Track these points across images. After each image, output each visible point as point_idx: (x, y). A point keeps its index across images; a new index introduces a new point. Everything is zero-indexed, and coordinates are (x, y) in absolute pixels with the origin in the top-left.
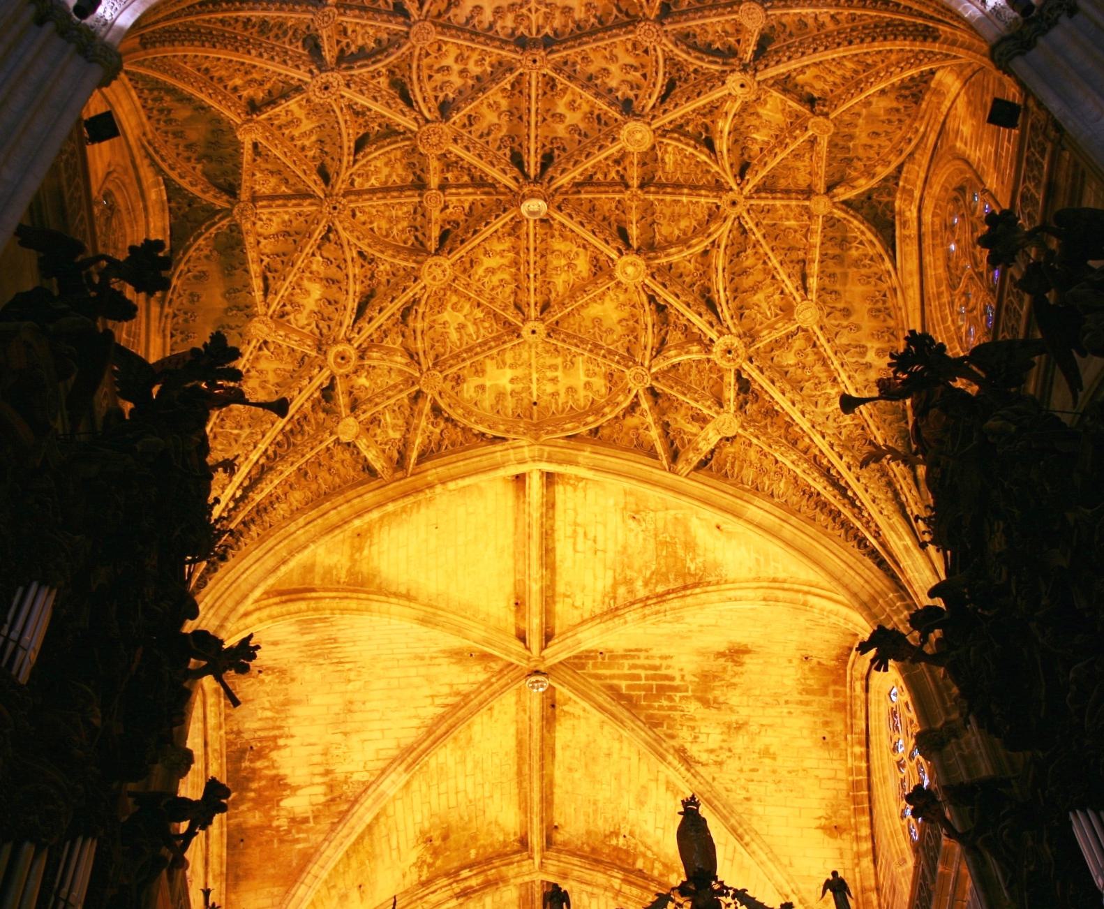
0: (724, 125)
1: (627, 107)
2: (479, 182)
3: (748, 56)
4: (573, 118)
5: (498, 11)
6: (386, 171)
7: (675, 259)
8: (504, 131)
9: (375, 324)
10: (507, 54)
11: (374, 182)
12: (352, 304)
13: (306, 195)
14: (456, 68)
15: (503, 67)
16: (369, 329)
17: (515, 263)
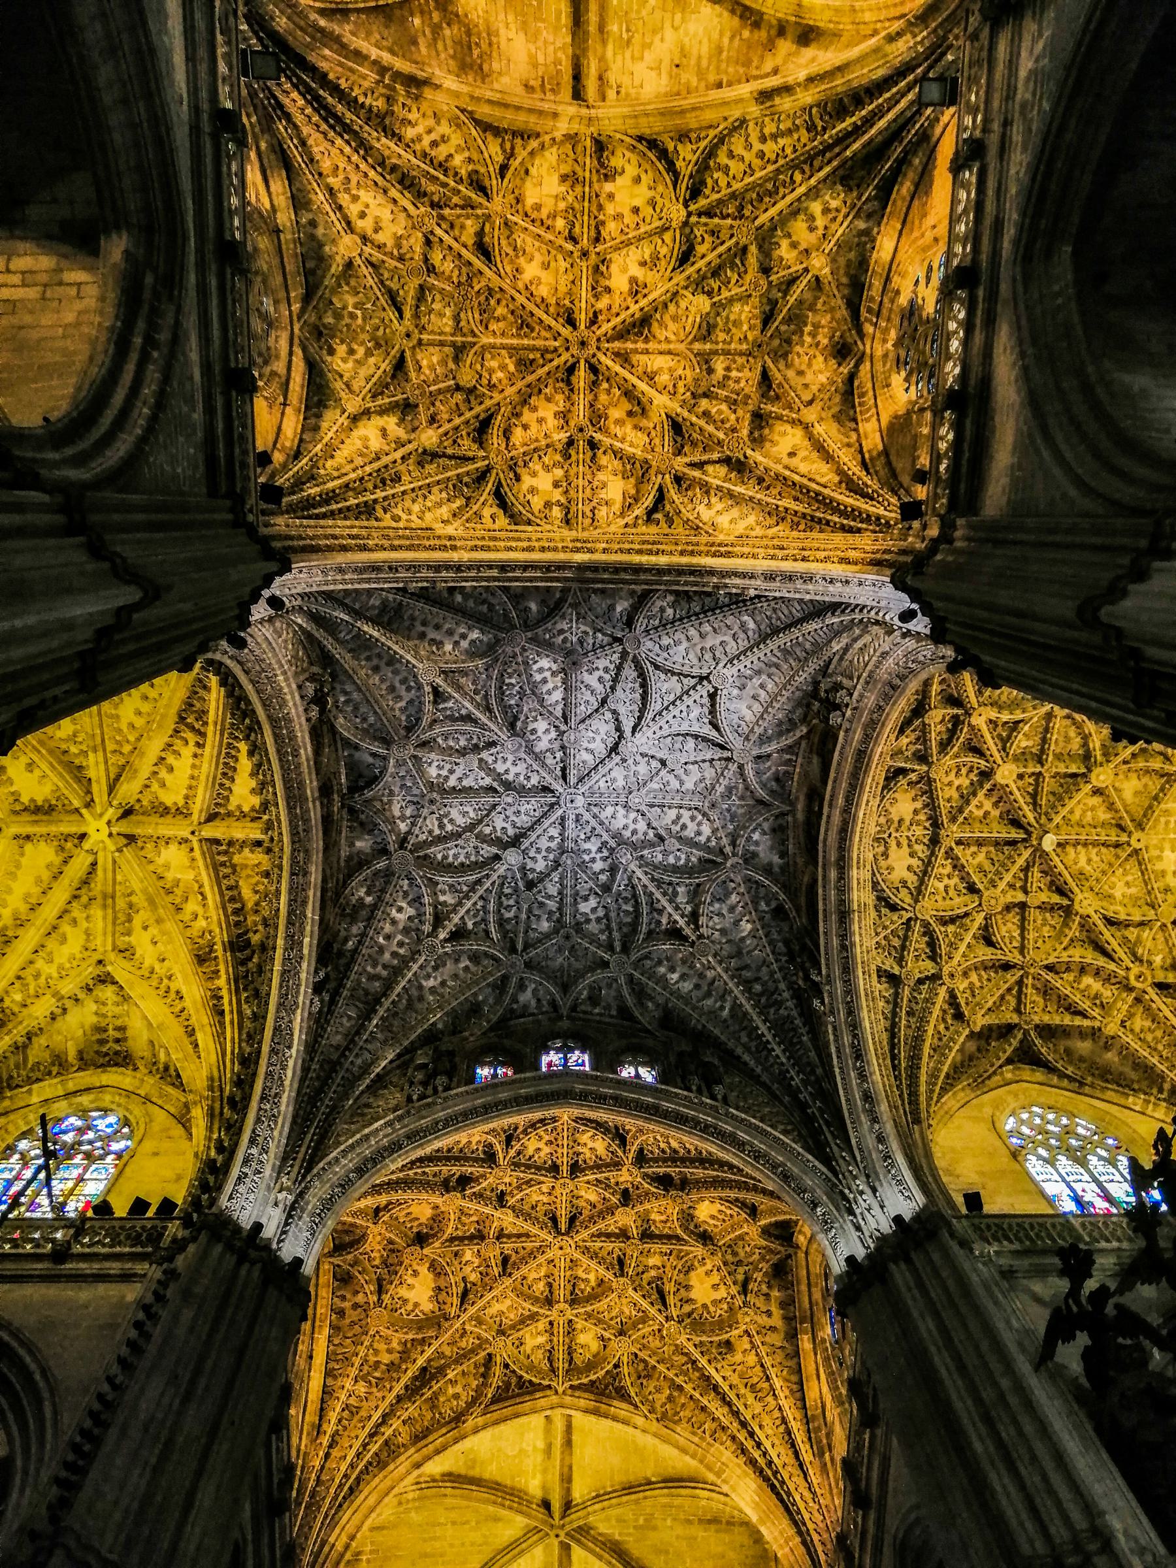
0: (1005, 717)
1: (986, 775)
2: (1026, 869)
3: (960, 712)
4: (988, 805)
5: (912, 855)
6: (1009, 925)
7: (1098, 745)
8: (992, 849)
9: (1117, 949)
10: (941, 854)
11: (1016, 934)
12: (1101, 961)
13: (1020, 983)
14: (946, 881)
15: (949, 853)
16: (1121, 953)
17: (1085, 845)
